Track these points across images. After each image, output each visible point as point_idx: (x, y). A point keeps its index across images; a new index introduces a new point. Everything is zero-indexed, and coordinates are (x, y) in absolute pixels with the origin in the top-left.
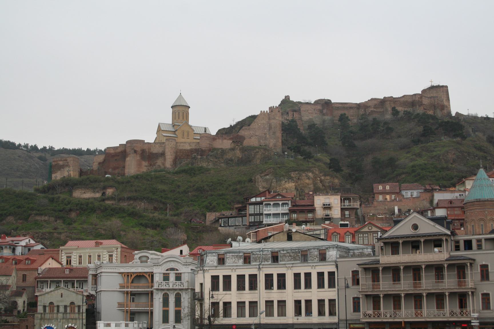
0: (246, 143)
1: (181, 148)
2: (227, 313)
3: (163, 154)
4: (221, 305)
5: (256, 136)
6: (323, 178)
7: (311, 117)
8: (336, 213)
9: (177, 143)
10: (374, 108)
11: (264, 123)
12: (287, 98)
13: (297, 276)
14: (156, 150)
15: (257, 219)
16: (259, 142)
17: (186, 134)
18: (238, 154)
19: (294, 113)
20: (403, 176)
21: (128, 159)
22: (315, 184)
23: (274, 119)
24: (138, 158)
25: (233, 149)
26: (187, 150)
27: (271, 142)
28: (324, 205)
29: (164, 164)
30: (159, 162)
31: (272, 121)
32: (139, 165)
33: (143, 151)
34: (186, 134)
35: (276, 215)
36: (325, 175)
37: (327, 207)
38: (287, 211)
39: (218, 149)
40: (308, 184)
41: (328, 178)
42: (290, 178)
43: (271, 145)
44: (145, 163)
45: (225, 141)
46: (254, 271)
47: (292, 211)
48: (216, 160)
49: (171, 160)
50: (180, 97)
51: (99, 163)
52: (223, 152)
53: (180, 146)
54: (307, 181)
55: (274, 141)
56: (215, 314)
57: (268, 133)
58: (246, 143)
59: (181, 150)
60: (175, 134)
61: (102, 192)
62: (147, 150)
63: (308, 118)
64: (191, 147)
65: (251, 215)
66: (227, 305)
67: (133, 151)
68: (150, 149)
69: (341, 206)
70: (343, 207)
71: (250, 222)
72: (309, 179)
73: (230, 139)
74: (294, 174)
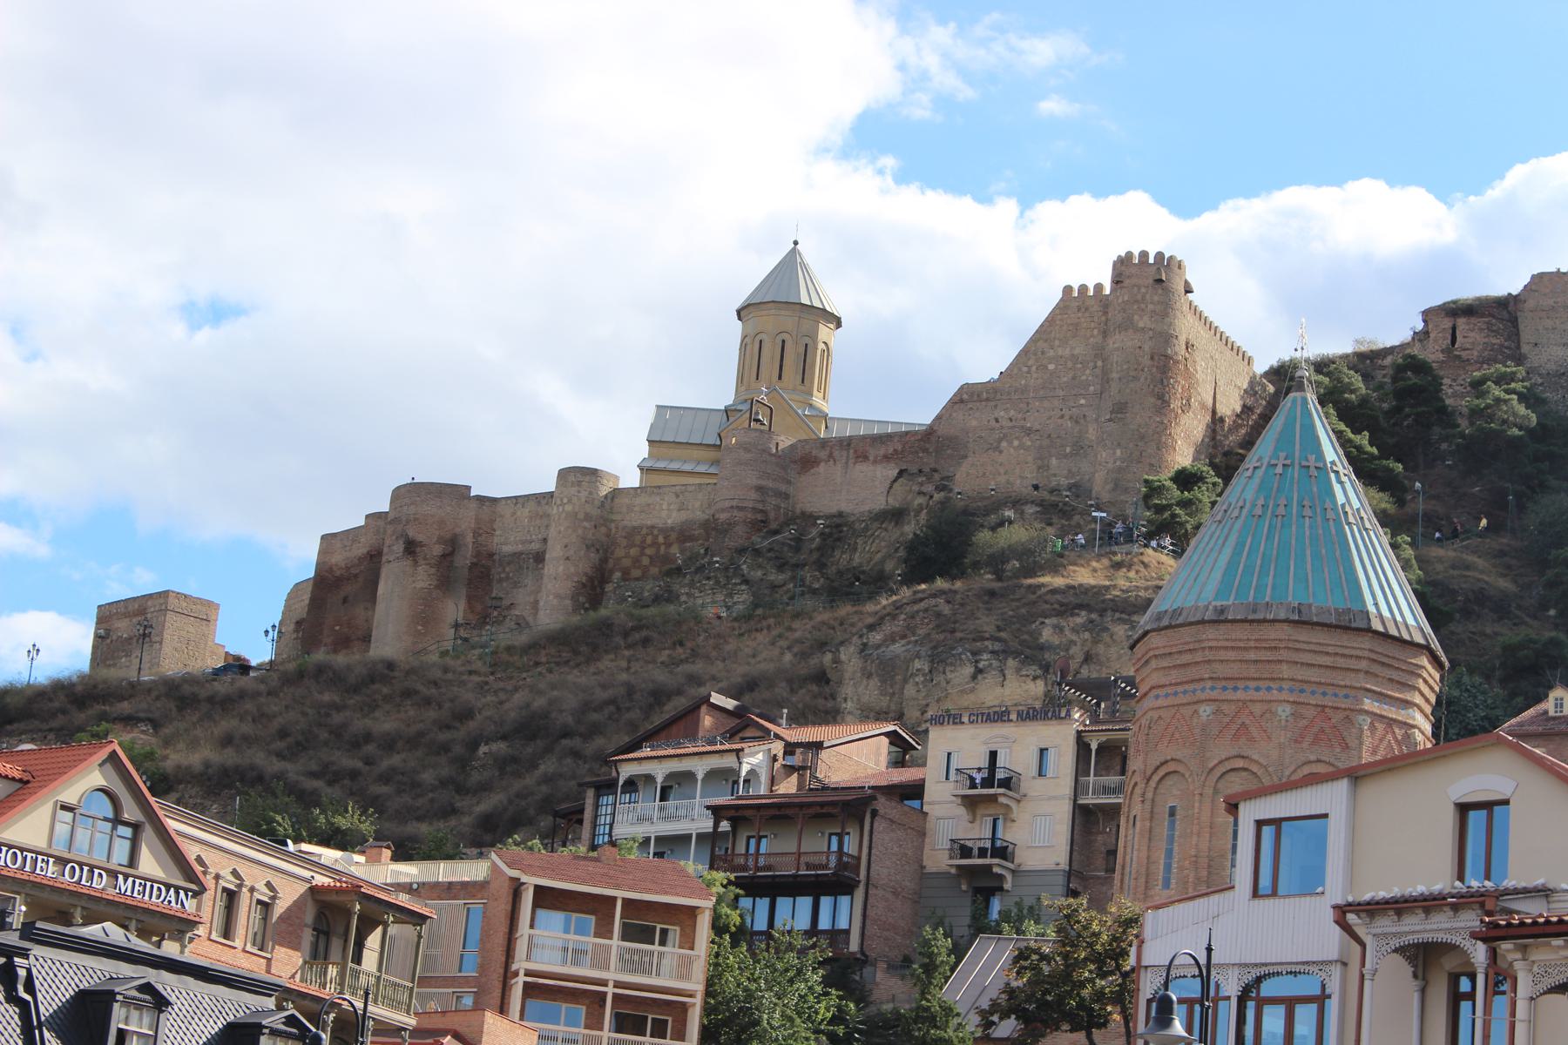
11: (1074, 358)
16: (1043, 468)
23: (1127, 325)
26: (666, 531)
31: (1117, 341)
33: (452, 544)
39: (810, 518)
48: (775, 577)
49: (566, 587)
50: (791, 264)
52: (839, 530)
53: (630, 508)
57: (1091, 415)
64: (684, 516)
69: (1078, 789)
70: (1089, 800)
74: (1059, 629)
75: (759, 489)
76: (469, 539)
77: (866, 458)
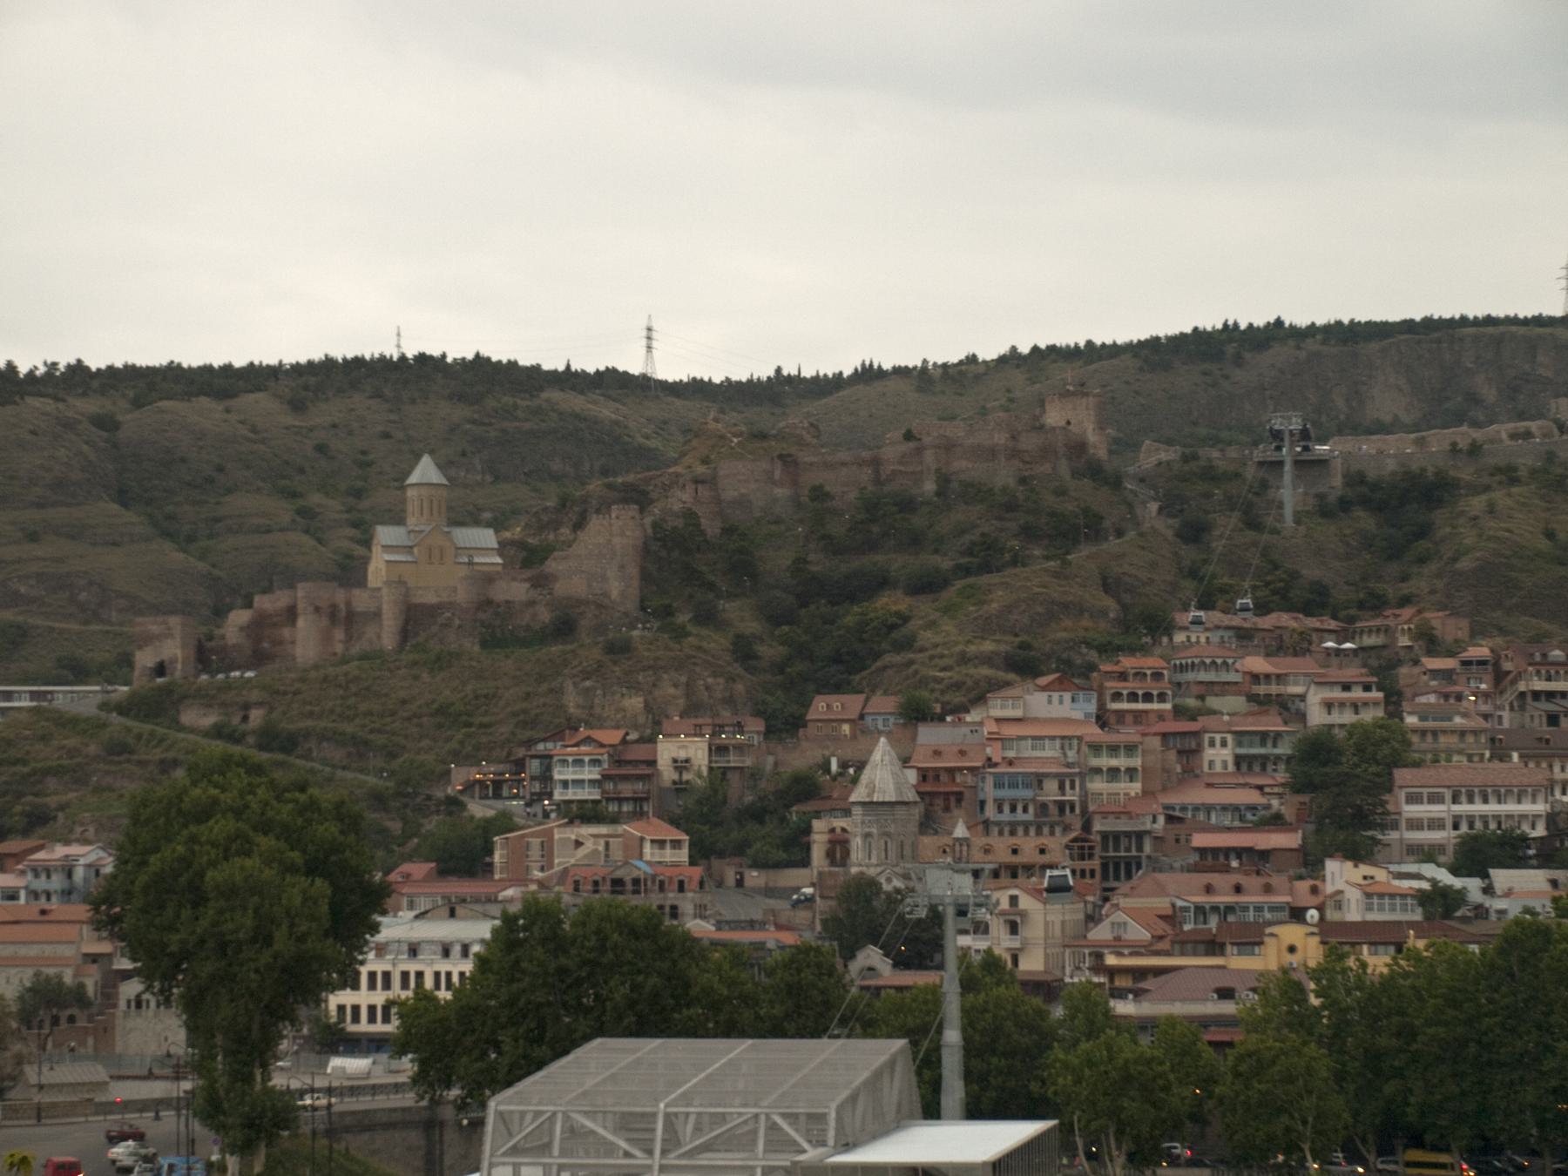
0: (560, 589)
1: (417, 600)
2: (356, 1018)
3: (377, 615)
4: (349, 1011)
6: (710, 680)
10: (900, 463)
13: (437, 974)
18: (545, 616)
19: (700, 487)
20: (890, 672)
21: (301, 623)
24: (325, 622)
25: (532, 603)
27: (615, 588)
28: (675, 761)
29: (379, 637)
30: (370, 631)
32: (327, 638)
35: (579, 783)
36: (714, 675)
37: (681, 765)
38: (598, 777)
40: (675, 697)
41: (721, 680)
42: (635, 688)
43: (615, 594)
45: (514, 584)
46: (388, 967)
47: (606, 777)
51: (241, 629)
54: (672, 691)
55: (620, 587)
56: (437, 986)
58: (560, 589)
59: (416, 606)
60: (411, 553)
61: (242, 713)
62: (342, 606)
66: (356, 1009)
67: (311, 609)
71: (532, 794)
72: (675, 686)
73: (525, 580)
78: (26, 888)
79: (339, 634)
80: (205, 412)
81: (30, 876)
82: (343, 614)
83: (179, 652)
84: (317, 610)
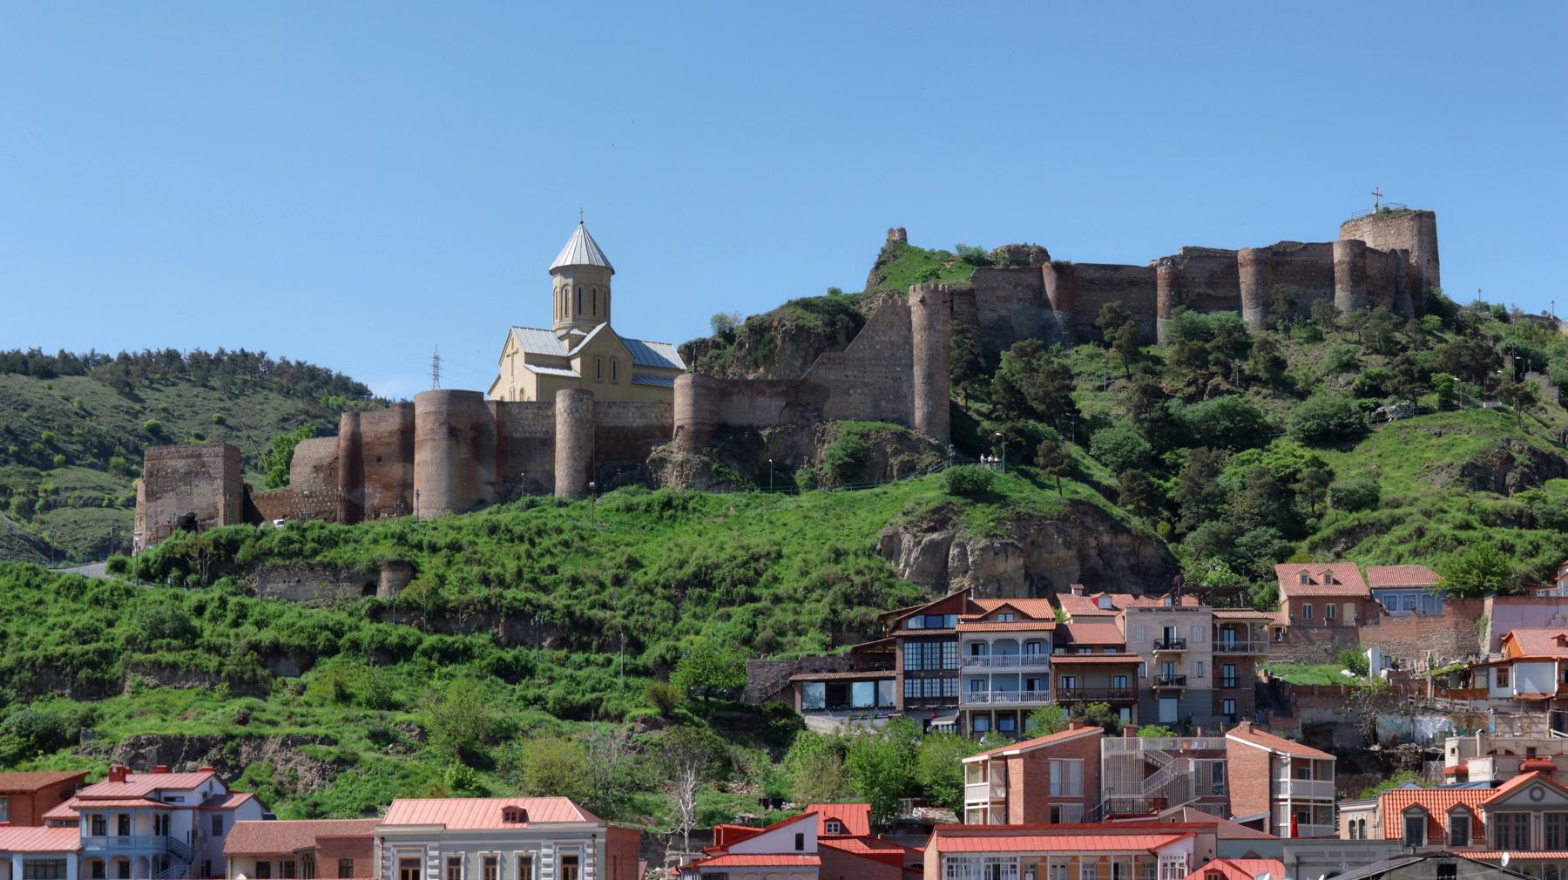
1: (610, 422)
3: (548, 442)
5: (866, 385)
6: (1106, 539)
7: (1003, 312)
8: (1198, 672)
9: (596, 404)
11: (892, 343)
12: (903, 231)
14: (525, 428)
15: (932, 688)
17: (607, 368)
22: (1083, 558)
24: (464, 452)
34: (607, 368)
44: (487, 473)
45: (762, 401)
51: (317, 469)
54: (1062, 553)
59: (609, 431)
62: (493, 428)
63: (994, 316)
64: (644, 421)
65: (908, 675)
68: (501, 424)
72: (1067, 544)
75: (711, 411)
76: (493, 428)
77: (764, 393)
78: (79, 852)
79: (487, 473)
80: (18, 384)
81: (85, 828)
82: (495, 442)
83: (220, 501)
84: (453, 433)
